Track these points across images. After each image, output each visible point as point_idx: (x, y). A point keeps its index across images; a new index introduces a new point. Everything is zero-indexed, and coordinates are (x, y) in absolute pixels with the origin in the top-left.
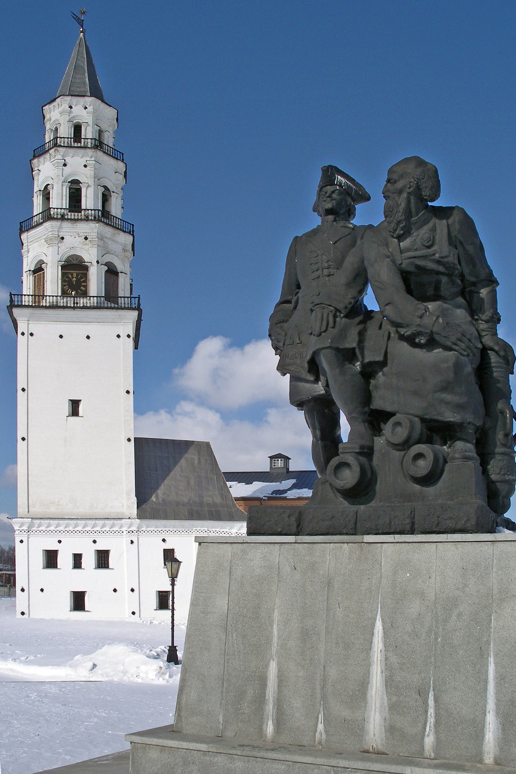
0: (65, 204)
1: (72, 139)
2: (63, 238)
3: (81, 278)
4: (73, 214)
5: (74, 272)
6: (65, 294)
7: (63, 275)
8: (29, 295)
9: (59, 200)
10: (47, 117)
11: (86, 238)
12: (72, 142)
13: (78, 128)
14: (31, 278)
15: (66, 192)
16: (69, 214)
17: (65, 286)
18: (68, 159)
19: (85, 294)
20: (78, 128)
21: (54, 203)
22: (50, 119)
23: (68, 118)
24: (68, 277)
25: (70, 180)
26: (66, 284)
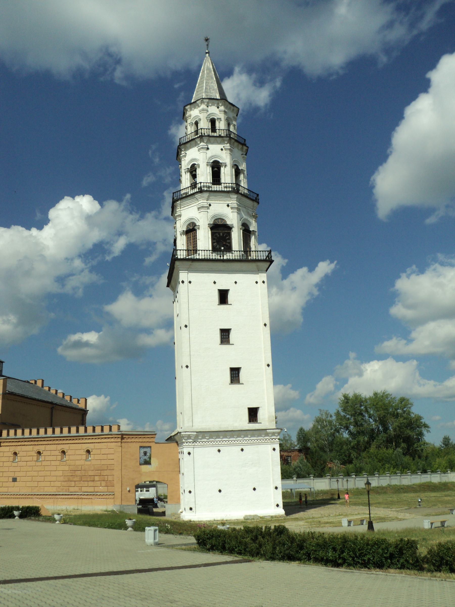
0: (209, 179)
1: (210, 130)
2: (210, 205)
3: (226, 236)
4: (215, 186)
5: (220, 231)
6: (215, 249)
7: (213, 234)
8: (183, 250)
9: (204, 176)
10: (188, 114)
11: (228, 206)
12: (210, 132)
13: (213, 122)
14: (184, 237)
15: (209, 170)
16: (213, 186)
17: (214, 243)
18: (210, 146)
19: (229, 249)
20: (213, 122)
21: (199, 179)
22: (190, 116)
23: (206, 115)
24: (216, 236)
25: (211, 161)
26: (215, 241)
